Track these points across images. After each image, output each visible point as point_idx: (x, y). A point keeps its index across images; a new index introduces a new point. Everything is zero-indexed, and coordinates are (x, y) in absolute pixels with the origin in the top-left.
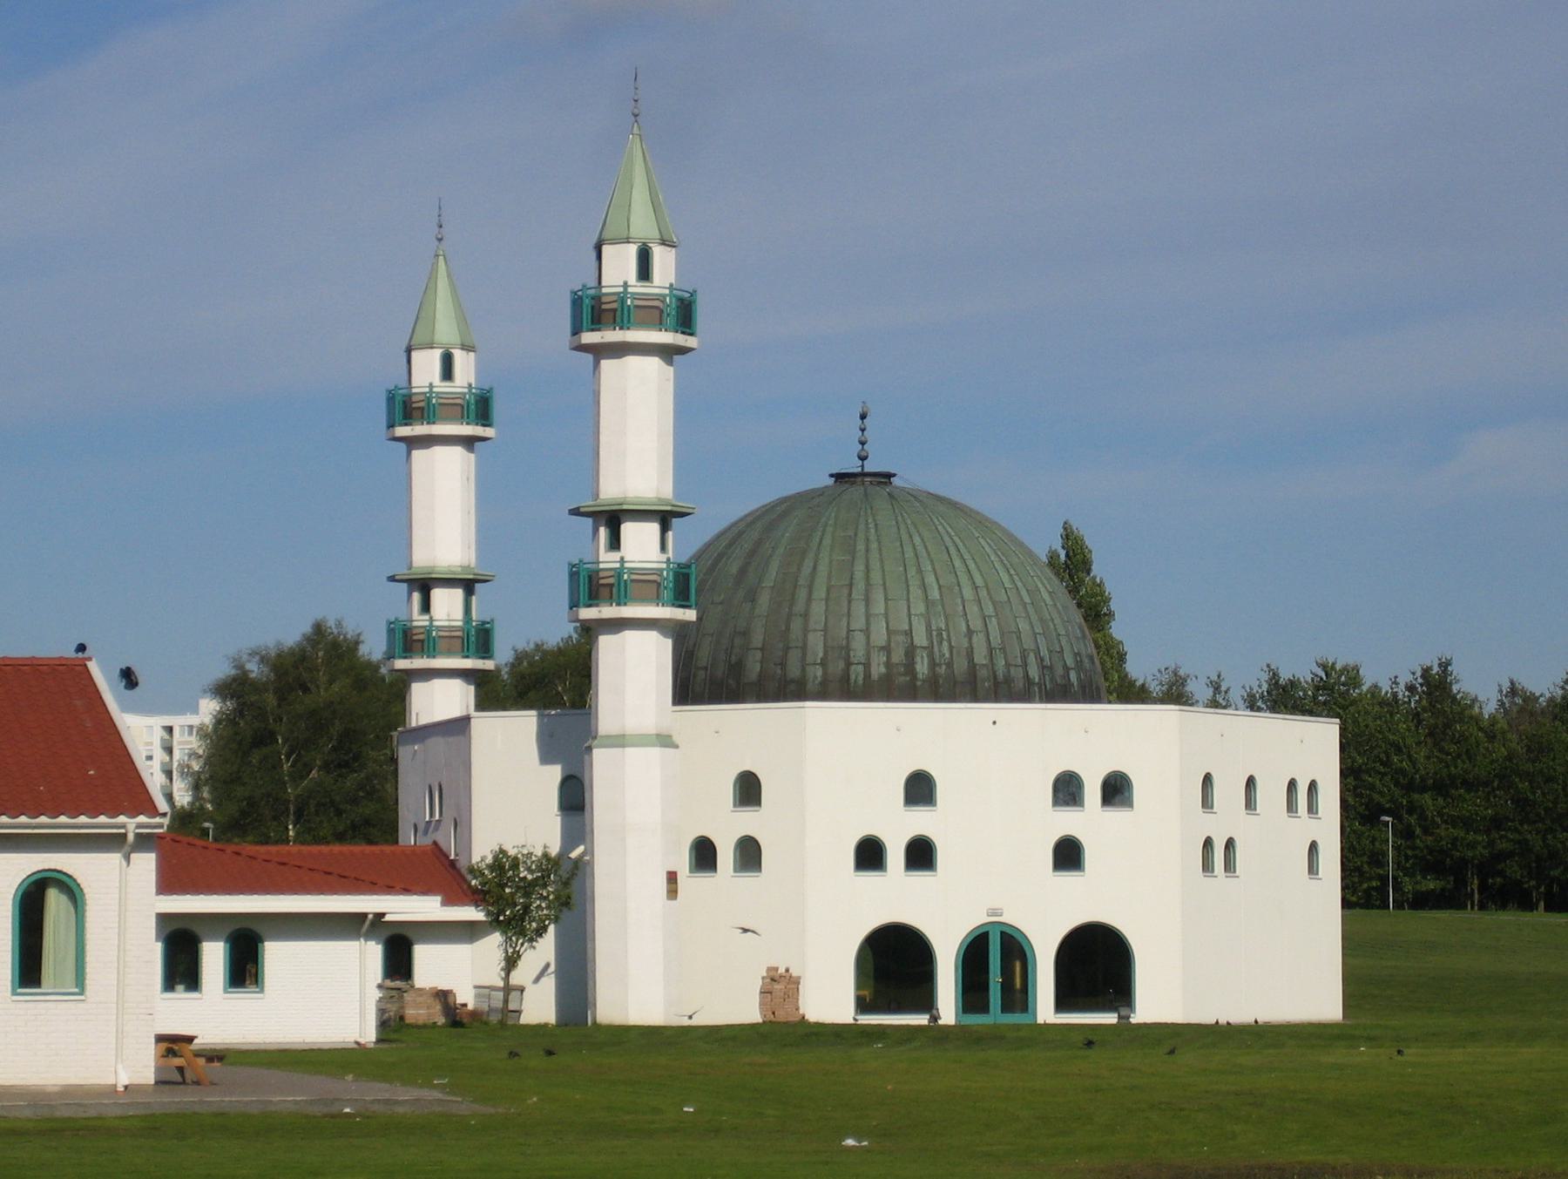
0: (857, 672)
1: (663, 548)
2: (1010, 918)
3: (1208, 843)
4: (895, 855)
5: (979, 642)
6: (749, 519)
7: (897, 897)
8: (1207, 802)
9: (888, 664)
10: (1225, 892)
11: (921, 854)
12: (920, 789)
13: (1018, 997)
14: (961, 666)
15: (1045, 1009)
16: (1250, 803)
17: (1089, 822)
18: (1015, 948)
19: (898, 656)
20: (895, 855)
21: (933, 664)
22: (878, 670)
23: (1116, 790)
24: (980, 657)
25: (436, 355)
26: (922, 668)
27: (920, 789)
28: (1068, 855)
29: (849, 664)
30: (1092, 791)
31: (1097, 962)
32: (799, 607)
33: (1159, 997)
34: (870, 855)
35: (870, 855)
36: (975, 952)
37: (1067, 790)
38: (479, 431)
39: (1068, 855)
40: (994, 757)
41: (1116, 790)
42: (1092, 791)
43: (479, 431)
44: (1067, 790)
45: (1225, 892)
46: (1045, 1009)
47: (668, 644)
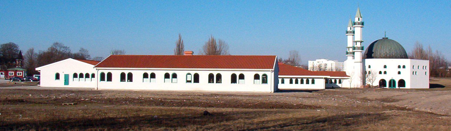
0: (382, 56)
1: (361, 45)
2: (394, 79)
3: (413, 72)
4: (383, 73)
5: (394, 53)
6: (154, 110)
7: (383, 77)
8: (413, 68)
9: (385, 55)
10: (413, 74)
11: (385, 73)
12: (385, 67)
13: (394, 86)
14: (392, 56)
15: (397, 87)
16: (426, 74)
17: (401, 70)
18: (394, 82)
19: (386, 54)
20: (383, 73)
21: (389, 55)
22: (384, 56)
23: (404, 67)
24: (394, 55)
25: (350, 27)
26: (388, 56)
27: (385, 67)
28: (399, 73)
29: (381, 55)
30: (402, 67)
31: (402, 83)
32: (376, 53)
33: (408, 86)
34: (380, 73)
35: (380, 73)
36: (390, 82)
37: (399, 67)
38: (354, 34)
39: (399, 73)
40: (393, 64)
41: (404, 67)
42: (402, 67)
43: (354, 34)
44: (399, 67)
45: (413, 74)
46: (397, 87)
47: (324, 80)
